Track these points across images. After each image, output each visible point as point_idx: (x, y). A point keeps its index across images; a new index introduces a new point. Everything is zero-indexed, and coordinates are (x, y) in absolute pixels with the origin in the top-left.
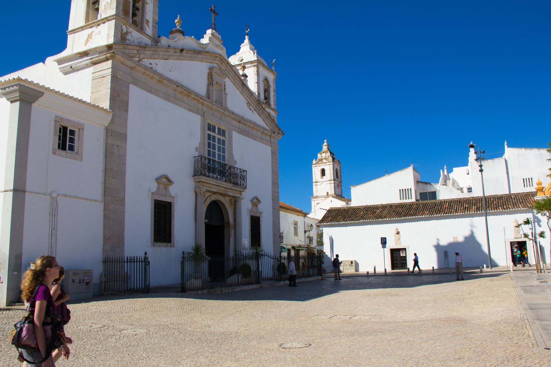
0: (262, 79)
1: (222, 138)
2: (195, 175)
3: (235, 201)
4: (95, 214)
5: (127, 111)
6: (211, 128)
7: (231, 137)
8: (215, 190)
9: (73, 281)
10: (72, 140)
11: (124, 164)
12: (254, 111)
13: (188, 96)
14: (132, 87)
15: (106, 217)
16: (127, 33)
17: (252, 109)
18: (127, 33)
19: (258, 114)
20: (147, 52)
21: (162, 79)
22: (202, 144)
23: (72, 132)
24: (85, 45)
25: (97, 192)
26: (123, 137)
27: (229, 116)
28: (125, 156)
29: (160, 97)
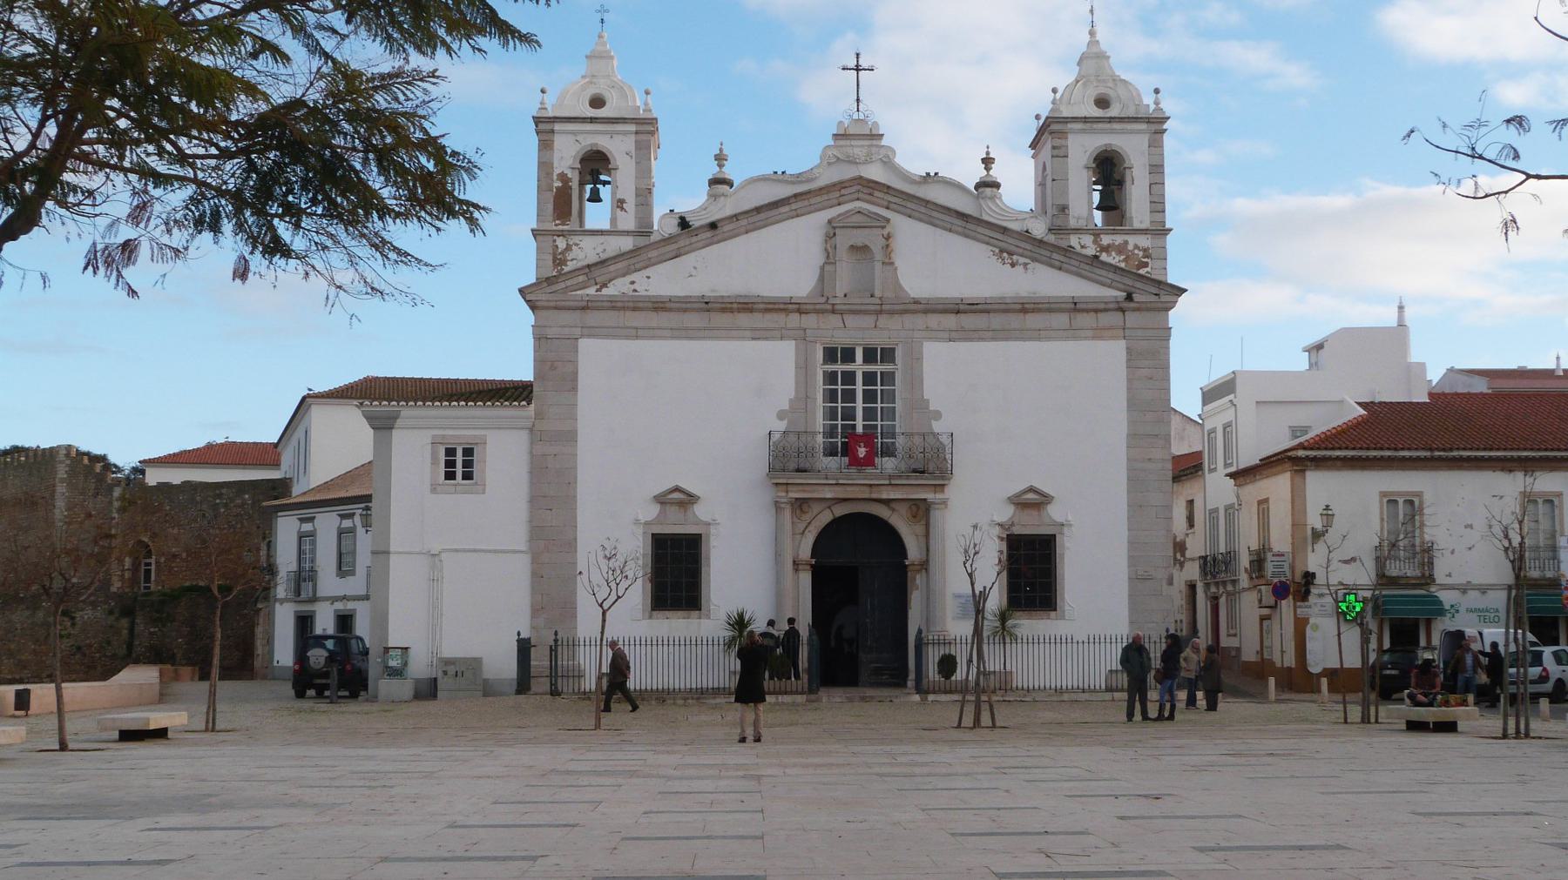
1: (878, 368)
2: (772, 469)
4: (519, 569)
5: (574, 389)
7: (916, 359)
8: (829, 496)
9: (445, 673)
10: (468, 464)
11: (571, 483)
12: (1032, 265)
13: (751, 311)
14: (583, 343)
15: (537, 576)
16: (569, 248)
17: (1022, 260)
18: (569, 248)
19: (1052, 266)
20: (612, 268)
21: (660, 305)
22: (802, 398)
23: (468, 452)
26: (571, 437)
27: (914, 312)
28: (575, 468)
29: (664, 338)
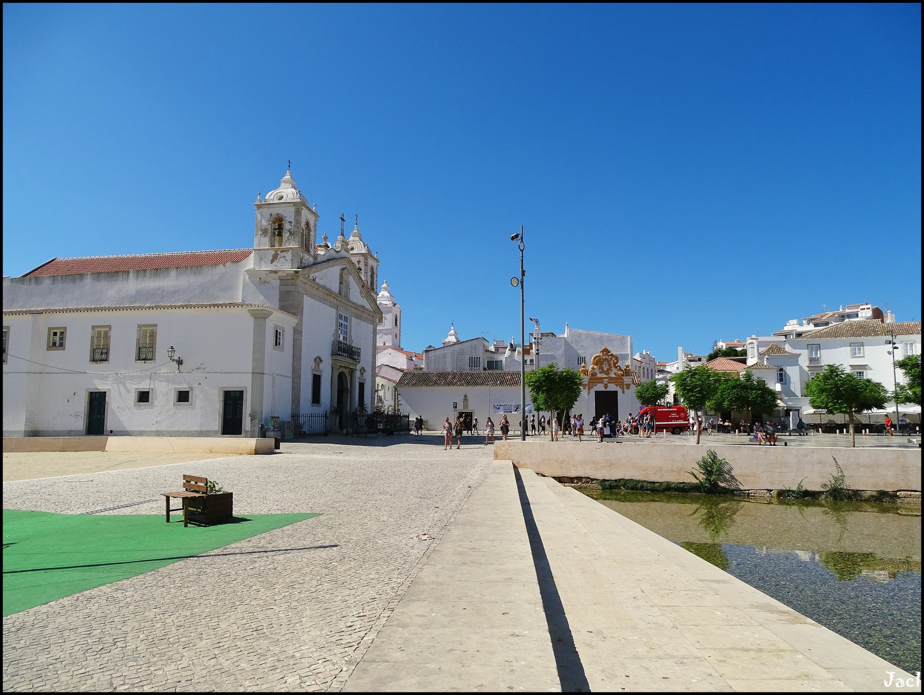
0: (369, 268)
3: (352, 372)
6: (341, 317)
24: (272, 261)
25: (289, 372)
26: (300, 333)
